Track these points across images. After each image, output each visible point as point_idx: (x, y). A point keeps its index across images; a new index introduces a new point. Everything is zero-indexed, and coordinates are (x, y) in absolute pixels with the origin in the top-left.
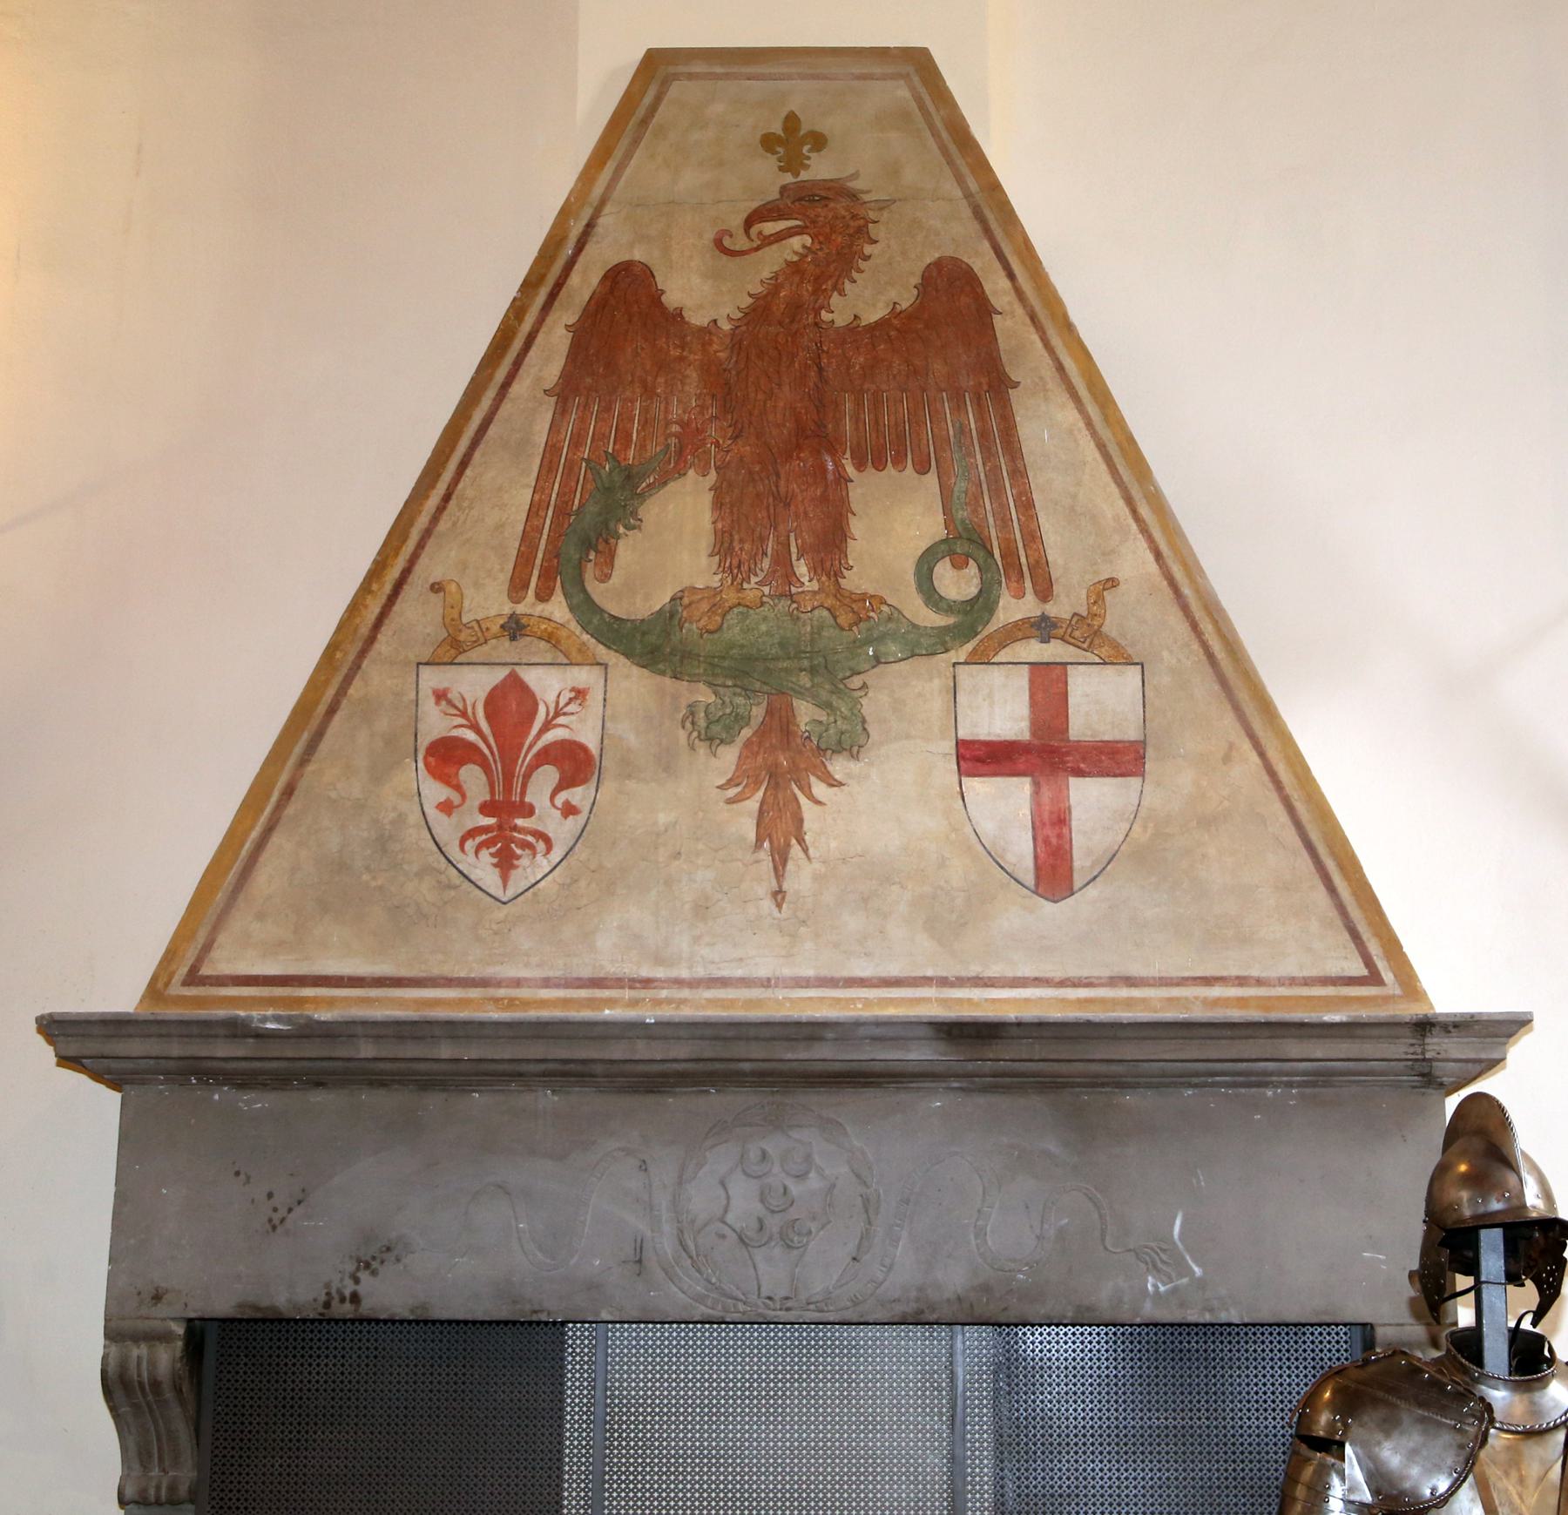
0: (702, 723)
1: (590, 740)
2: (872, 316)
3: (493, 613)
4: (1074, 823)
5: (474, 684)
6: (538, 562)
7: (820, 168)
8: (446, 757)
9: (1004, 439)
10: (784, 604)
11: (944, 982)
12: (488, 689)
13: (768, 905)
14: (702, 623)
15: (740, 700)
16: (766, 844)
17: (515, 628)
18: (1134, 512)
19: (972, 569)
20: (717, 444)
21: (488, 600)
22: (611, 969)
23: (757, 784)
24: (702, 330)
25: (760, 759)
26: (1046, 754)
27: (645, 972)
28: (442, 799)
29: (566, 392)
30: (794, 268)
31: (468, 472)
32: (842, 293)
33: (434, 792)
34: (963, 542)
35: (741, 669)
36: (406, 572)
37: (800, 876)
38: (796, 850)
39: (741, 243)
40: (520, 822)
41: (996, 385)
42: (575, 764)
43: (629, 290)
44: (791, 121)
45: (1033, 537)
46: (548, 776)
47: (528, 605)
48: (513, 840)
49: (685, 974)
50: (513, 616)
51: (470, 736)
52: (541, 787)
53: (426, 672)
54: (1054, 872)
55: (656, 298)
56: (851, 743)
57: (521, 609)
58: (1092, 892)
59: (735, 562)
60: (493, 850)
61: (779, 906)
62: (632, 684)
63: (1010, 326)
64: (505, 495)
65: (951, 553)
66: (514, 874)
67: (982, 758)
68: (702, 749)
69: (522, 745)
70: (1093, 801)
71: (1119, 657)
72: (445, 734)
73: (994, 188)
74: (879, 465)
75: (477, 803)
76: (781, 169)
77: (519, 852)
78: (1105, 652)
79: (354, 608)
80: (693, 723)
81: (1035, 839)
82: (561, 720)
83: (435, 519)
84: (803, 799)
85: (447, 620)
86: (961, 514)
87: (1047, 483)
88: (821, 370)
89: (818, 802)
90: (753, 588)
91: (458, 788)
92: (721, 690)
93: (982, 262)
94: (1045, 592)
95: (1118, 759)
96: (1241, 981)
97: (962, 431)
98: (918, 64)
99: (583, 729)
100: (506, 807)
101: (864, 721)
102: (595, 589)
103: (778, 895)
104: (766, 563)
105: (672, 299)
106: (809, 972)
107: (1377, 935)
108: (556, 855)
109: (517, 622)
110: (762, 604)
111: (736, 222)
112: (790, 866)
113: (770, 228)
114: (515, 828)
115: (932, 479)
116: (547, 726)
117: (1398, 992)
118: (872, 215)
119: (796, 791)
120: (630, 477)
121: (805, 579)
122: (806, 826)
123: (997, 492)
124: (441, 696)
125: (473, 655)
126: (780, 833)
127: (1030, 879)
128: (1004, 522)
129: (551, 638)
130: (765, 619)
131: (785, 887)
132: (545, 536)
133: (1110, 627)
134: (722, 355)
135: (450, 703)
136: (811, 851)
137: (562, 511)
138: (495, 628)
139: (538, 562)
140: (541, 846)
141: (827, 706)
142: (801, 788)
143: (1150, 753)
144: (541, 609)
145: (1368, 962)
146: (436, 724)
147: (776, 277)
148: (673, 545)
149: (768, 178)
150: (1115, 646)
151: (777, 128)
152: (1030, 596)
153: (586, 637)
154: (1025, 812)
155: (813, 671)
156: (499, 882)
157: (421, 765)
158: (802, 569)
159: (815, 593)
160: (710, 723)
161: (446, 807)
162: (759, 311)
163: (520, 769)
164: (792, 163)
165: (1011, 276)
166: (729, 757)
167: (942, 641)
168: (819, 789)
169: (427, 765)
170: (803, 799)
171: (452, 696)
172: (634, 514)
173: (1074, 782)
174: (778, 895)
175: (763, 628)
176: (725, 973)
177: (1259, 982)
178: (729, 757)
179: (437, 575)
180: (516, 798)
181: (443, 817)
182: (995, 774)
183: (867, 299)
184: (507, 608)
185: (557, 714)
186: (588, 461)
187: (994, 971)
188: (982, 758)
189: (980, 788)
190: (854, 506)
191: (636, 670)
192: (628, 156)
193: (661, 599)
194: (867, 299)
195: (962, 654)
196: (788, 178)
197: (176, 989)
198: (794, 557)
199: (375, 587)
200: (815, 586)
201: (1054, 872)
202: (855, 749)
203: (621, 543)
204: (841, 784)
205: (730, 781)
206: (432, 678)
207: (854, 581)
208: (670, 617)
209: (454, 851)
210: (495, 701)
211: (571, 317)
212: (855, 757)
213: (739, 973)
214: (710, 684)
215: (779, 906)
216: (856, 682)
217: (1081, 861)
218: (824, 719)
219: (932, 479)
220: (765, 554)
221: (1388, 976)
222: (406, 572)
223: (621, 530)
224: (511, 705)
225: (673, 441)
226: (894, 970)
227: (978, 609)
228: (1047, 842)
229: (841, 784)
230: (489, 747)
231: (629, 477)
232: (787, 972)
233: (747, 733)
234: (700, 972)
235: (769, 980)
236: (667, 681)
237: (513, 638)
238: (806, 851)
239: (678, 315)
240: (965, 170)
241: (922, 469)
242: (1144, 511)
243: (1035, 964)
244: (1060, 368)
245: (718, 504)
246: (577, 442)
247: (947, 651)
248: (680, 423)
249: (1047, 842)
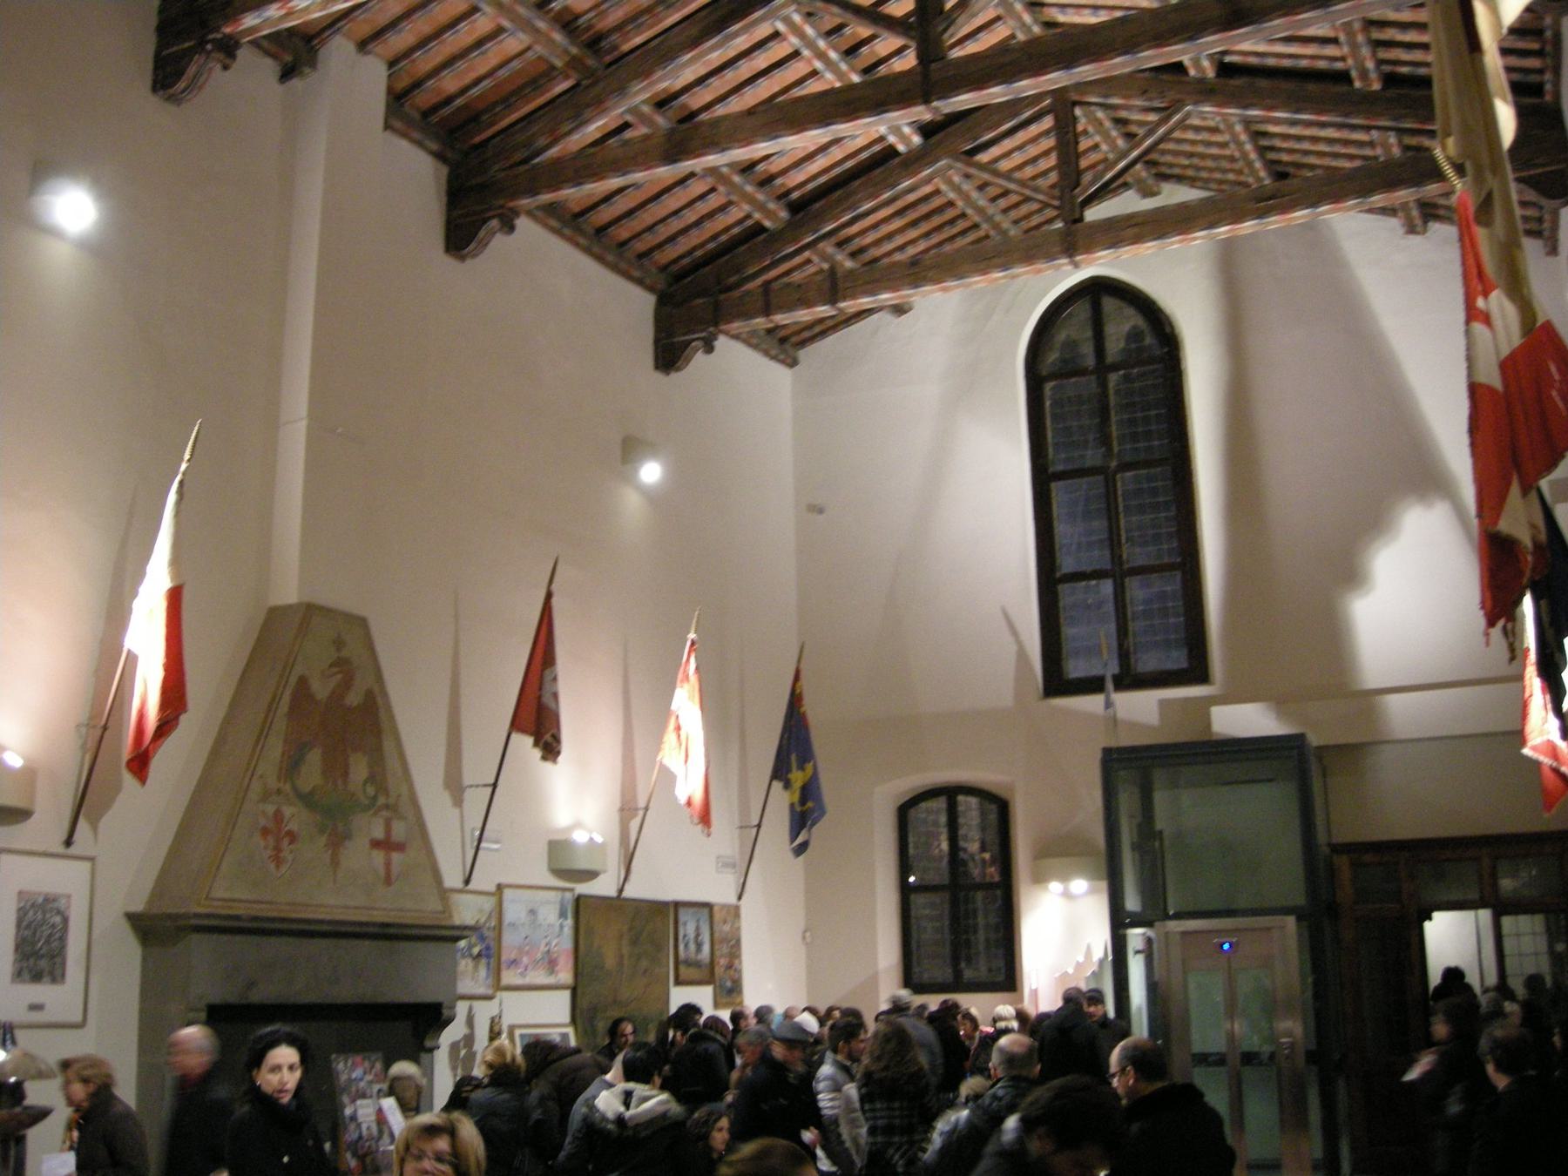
5: (270, 809)
7: (345, 653)
9: (379, 748)
21: (273, 783)
26: (386, 845)
33: (262, 843)
34: (371, 779)
41: (378, 733)
42: (292, 837)
46: (286, 841)
54: (388, 881)
56: (348, 836)
64: (275, 749)
67: (376, 844)
70: (396, 857)
93: (376, 689)
94: (388, 795)
95: (400, 847)
98: (362, 623)
99: (293, 826)
100: (278, 849)
126: (335, 862)
146: (263, 822)
148: (312, 773)
164: (339, 650)
167: (368, 808)
188: (376, 844)
208: (312, 793)
224: (278, 817)
227: (375, 798)
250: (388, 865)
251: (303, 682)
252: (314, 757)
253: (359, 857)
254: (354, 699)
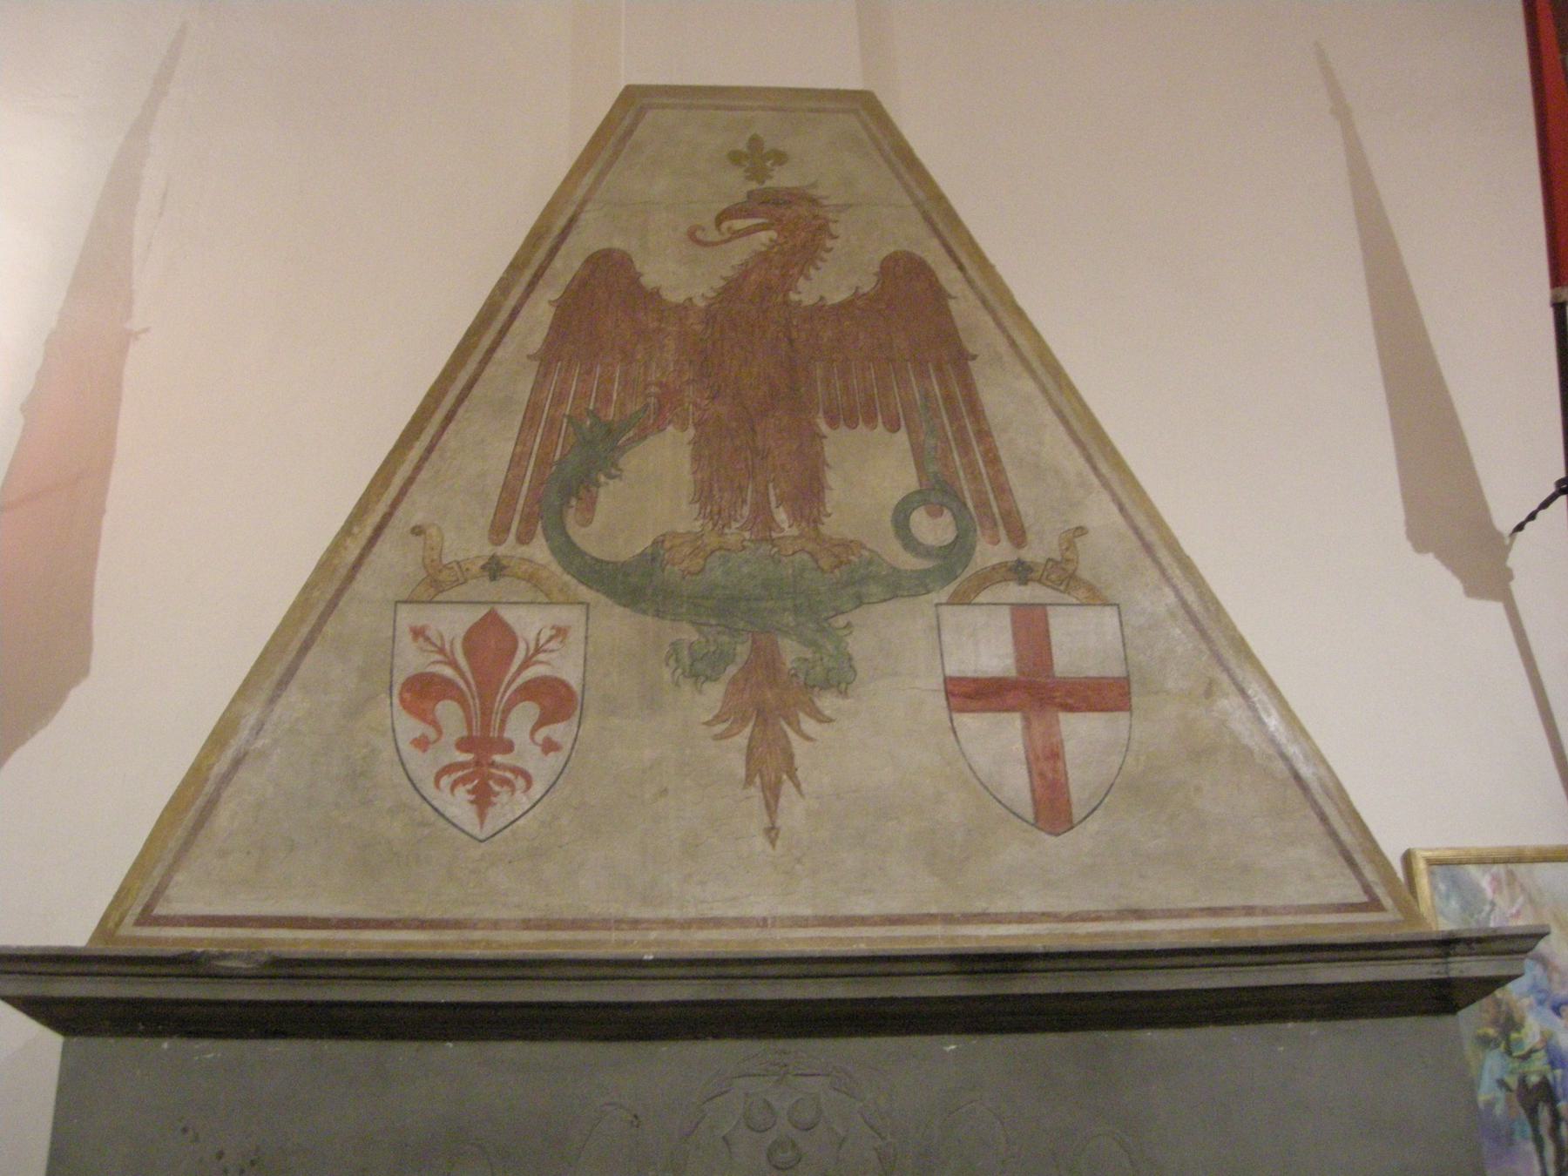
0: (687, 661)
1: (571, 675)
2: (838, 297)
3: (474, 553)
4: (1068, 757)
6: (519, 507)
7: (783, 179)
8: (423, 692)
10: (765, 548)
11: (948, 919)
12: (468, 625)
13: (760, 842)
14: (685, 565)
15: (725, 639)
16: (757, 780)
17: (494, 569)
18: (1095, 469)
19: (947, 518)
20: (695, 405)
21: (467, 543)
22: (597, 908)
23: (744, 720)
24: (678, 308)
25: (746, 696)
26: (1034, 690)
27: (633, 913)
28: (418, 734)
29: (548, 358)
30: (763, 257)
31: (452, 426)
32: (808, 278)
33: (410, 728)
34: (937, 491)
35: (723, 608)
36: (388, 517)
37: (794, 811)
38: (787, 787)
39: (713, 235)
40: (498, 758)
41: (953, 357)
42: (555, 700)
43: (608, 278)
44: (755, 142)
45: (1002, 490)
47: (509, 548)
48: (491, 776)
49: (674, 913)
50: (493, 557)
51: (448, 672)
52: (520, 723)
53: (404, 611)
54: (1053, 808)
55: (635, 279)
56: (839, 678)
57: (501, 550)
58: (1092, 826)
59: (716, 509)
60: (469, 787)
61: (773, 843)
62: (617, 623)
63: (964, 307)
64: (487, 448)
65: (925, 502)
66: (491, 811)
67: (972, 694)
68: (687, 687)
69: (500, 681)
70: (1081, 733)
71: (1096, 597)
72: (420, 670)
73: (939, 198)
74: (852, 425)
75: (455, 738)
76: (748, 178)
77: (497, 788)
78: (1082, 594)
79: (335, 548)
80: (677, 660)
81: (1030, 772)
82: (541, 657)
83: (418, 469)
84: (792, 735)
85: (427, 561)
86: (933, 468)
87: (1012, 442)
88: (791, 341)
89: (808, 738)
90: (733, 534)
91: (434, 723)
92: (705, 629)
94: (1018, 536)
95: (1105, 695)
96: (1249, 911)
97: (926, 396)
100: (483, 743)
101: (850, 659)
102: (577, 533)
103: (772, 832)
104: (746, 511)
105: (650, 279)
106: (807, 911)
107: (1372, 861)
108: (538, 789)
109: (498, 564)
110: (744, 548)
111: (708, 221)
112: (783, 801)
113: (740, 224)
114: (493, 764)
115: (902, 436)
116: (526, 664)
117: (1399, 916)
118: (830, 216)
119: (786, 727)
120: (611, 432)
121: (785, 525)
122: (798, 761)
123: (965, 449)
124: (418, 633)
125: (453, 594)
126: (771, 771)
127: (1030, 817)
128: (974, 476)
129: (533, 579)
130: (747, 561)
131: (779, 823)
132: (526, 484)
133: (1084, 573)
134: (698, 328)
135: (427, 639)
136: (804, 786)
137: (543, 462)
138: (475, 569)
139: (519, 507)
140: (520, 783)
141: (812, 644)
142: (789, 724)
143: (1135, 688)
144: (524, 551)
145: (1367, 889)
146: (413, 660)
147: (747, 263)
148: (653, 493)
149: (736, 185)
150: (1091, 589)
151: (742, 146)
152: (1005, 544)
153: (567, 578)
154: (1018, 747)
155: (796, 610)
156: (477, 821)
157: (396, 700)
158: (781, 516)
159: (795, 538)
160: (694, 661)
161: (422, 743)
162: (731, 290)
163: (499, 705)
165: (961, 268)
166: (715, 693)
167: (919, 584)
168: (808, 725)
169: (402, 701)
170: (792, 735)
171: (432, 633)
172: (615, 465)
173: (1064, 717)
174: (772, 832)
175: (745, 570)
176: (718, 911)
177: (1266, 911)
178: (715, 693)
179: (418, 518)
180: (494, 734)
181: (417, 752)
182: (983, 710)
183: (830, 283)
184: (489, 550)
185: (538, 651)
186: (570, 417)
187: (1000, 906)
188: (972, 694)
189: (970, 723)
190: (829, 460)
191: (619, 610)
192: (610, 165)
193: (642, 544)
194: (830, 283)
195: (943, 595)
196: (754, 186)
197: (128, 929)
198: (773, 504)
199: (356, 530)
200: (795, 531)
201: (1053, 808)
202: (843, 686)
203: (602, 491)
204: (830, 720)
205: (717, 717)
206: (408, 617)
207: (833, 526)
208: (652, 558)
209: (429, 789)
210: (472, 640)
211: (555, 295)
212: (844, 694)
213: (732, 913)
214: (693, 623)
215: (773, 843)
216: (841, 621)
217: (1076, 793)
218: (809, 656)
219: (902, 436)
220: (744, 501)
221: (1387, 902)
222: (388, 517)
223: (602, 479)
224: (490, 642)
225: (653, 400)
226: (895, 907)
227: (954, 556)
228: (1042, 775)
229: (830, 720)
230: (467, 682)
231: (609, 431)
232: (784, 910)
233: (732, 670)
234: (692, 913)
235: (765, 920)
236: (649, 619)
237: (493, 578)
238: (798, 786)
239: (655, 295)
240: (913, 184)
241: (893, 427)
242: (1104, 468)
243: (1037, 897)
244: (1013, 343)
245: (696, 458)
246: (559, 399)
247: (928, 592)
248: (660, 385)
249: (1042, 775)
250: (1047, 764)
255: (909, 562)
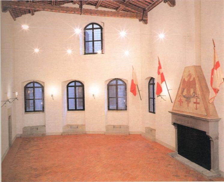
5: (180, 98)
34: (194, 92)
54: (196, 109)
56: (190, 102)
67: (194, 103)
70: (198, 105)
95: (199, 103)
100: (181, 104)
126: (188, 106)
146: (179, 100)
162: (188, 80)
188: (194, 103)
224: (181, 99)
227: (195, 95)
250: (196, 106)
251: (184, 79)
252: (185, 90)
253: (192, 105)
254: (191, 80)
255: (193, 96)
